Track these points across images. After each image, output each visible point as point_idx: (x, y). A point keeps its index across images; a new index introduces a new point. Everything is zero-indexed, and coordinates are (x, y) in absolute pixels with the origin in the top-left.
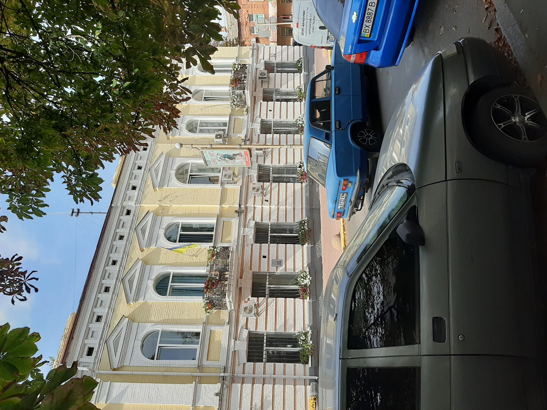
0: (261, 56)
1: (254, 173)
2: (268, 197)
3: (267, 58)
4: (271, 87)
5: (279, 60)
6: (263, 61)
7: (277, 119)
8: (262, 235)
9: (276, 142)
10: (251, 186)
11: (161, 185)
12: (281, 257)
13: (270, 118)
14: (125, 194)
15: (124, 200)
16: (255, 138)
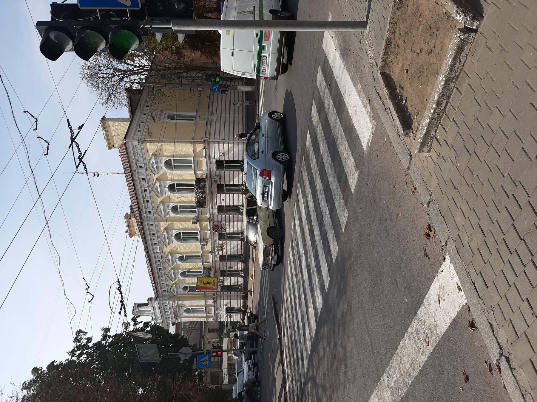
0: (213, 156)
1: (217, 238)
2: (225, 247)
3: (217, 157)
4: (223, 182)
5: (226, 158)
6: (214, 160)
7: (228, 204)
8: (222, 258)
9: (228, 219)
10: (216, 245)
11: (169, 244)
12: (232, 266)
13: (223, 204)
14: (153, 248)
15: (153, 250)
16: (215, 217)
